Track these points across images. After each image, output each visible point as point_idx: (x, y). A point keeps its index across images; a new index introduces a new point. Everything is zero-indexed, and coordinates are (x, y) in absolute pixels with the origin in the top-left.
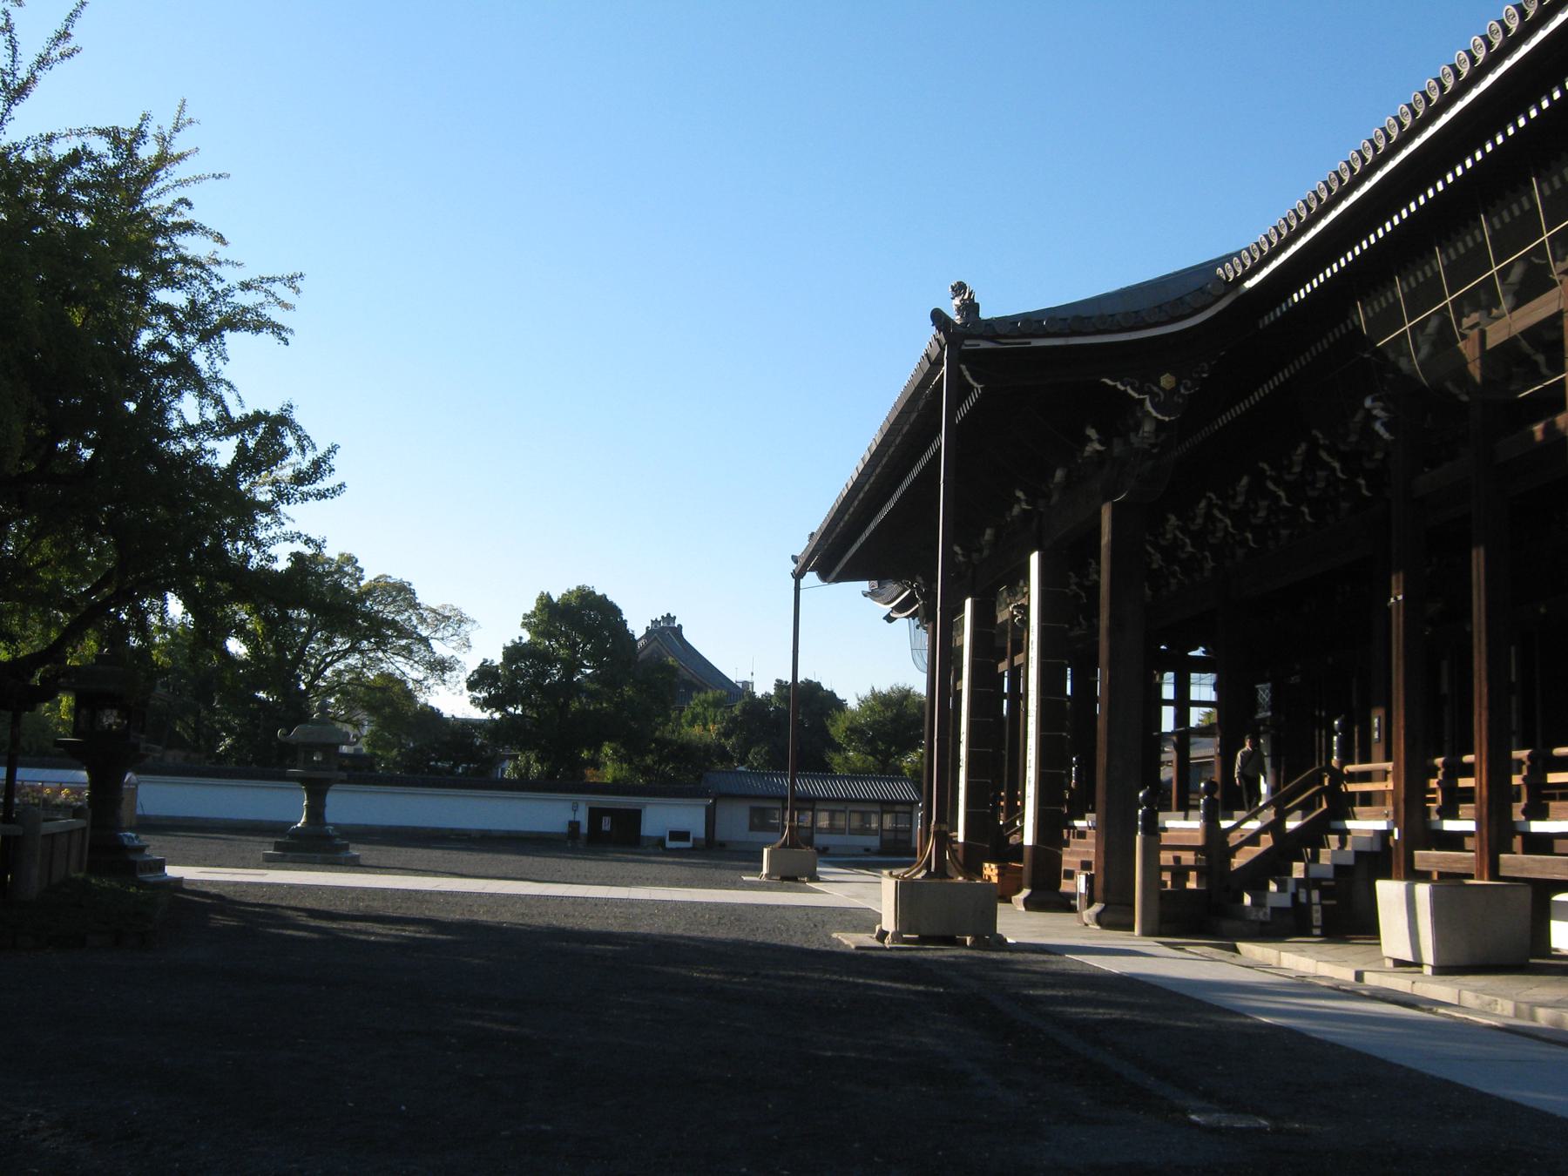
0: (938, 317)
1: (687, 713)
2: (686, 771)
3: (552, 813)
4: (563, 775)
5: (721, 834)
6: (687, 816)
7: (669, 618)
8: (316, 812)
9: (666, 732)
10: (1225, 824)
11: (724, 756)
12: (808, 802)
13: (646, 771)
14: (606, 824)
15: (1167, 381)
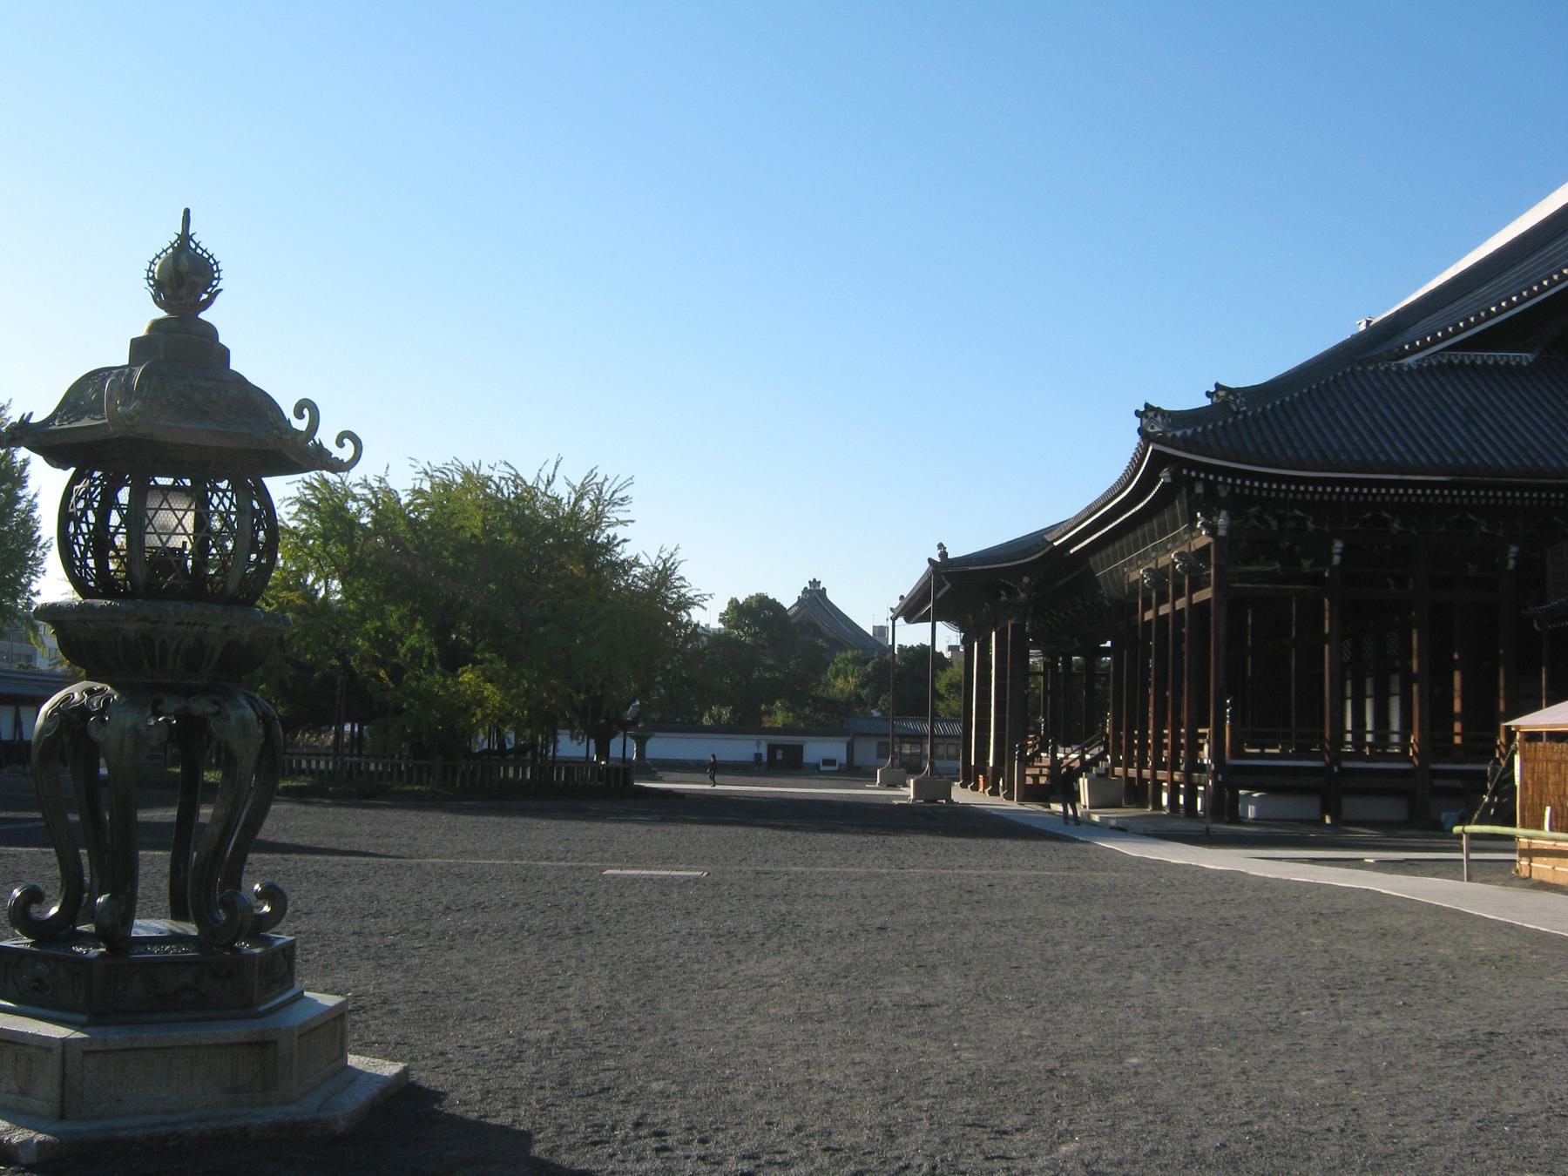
0: (930, 560)
1: (832, 669)
2: (833, 717)
3: (742, 748)
4: (746, 722)
5: (857, 762)
6: (835, 749)
7: (815, 583)
8: (641, 752)
9: (819, 692)
10: (1060, 755)
11: (859, 701)
12: (917, 738)
13: (805, 718)
14: (779, 755)
15: (1026, 580)
